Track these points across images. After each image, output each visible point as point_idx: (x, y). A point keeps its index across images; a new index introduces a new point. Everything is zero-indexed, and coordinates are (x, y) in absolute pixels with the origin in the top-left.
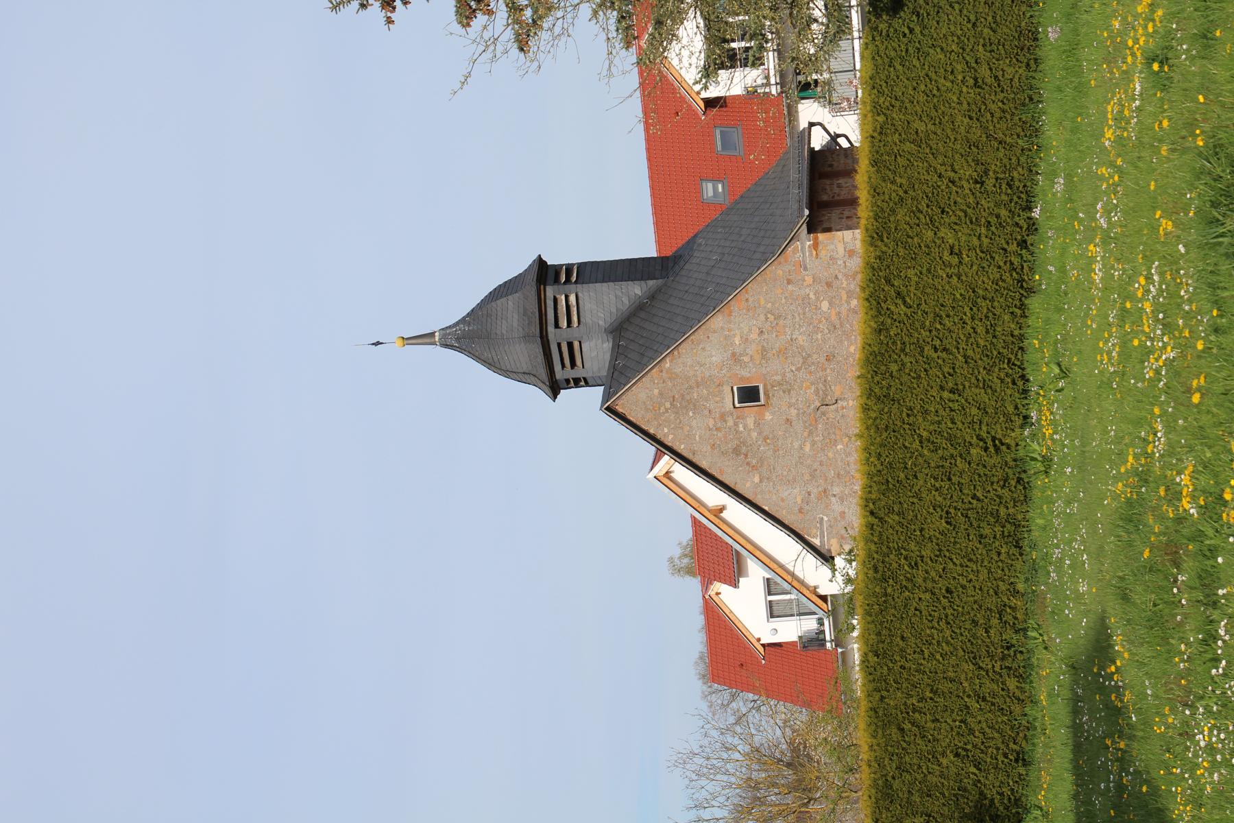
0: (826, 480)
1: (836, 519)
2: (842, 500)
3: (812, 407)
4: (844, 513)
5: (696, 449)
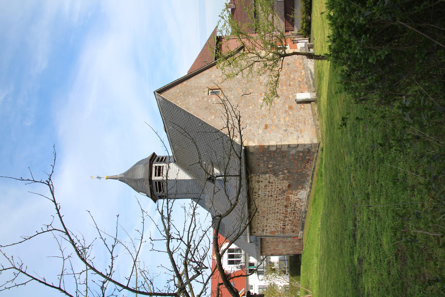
0: (244, 118)
1: (247, 132)
4: (251, 130)
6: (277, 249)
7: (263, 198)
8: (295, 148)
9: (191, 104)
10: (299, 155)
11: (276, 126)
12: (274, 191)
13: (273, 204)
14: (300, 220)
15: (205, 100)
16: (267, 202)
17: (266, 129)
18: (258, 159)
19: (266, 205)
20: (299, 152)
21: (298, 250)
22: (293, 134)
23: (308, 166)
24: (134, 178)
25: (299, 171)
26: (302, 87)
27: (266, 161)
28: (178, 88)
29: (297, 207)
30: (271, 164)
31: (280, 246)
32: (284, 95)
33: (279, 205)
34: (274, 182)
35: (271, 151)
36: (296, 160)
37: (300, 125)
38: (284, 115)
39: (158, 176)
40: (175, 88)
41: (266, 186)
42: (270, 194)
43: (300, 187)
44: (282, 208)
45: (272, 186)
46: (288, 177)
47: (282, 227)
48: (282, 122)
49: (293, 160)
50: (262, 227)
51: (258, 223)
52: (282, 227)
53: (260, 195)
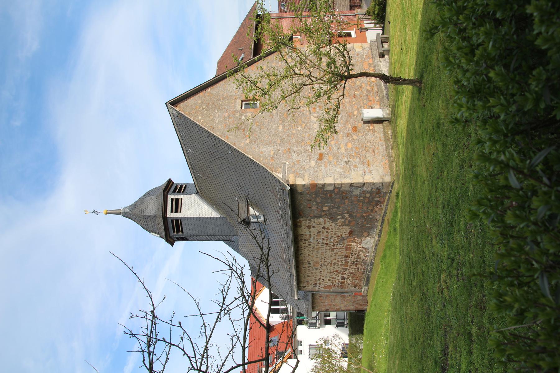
1: (294, 164)
2: (299, 154)
3: (286, 109)
4: (300, 161)
5: (215, 126)
6: (334, 303)
7: (316, 247)
8: (360, 187)
9: (217, 122)
10: (365, 196)
11: (335, 156)
12: (331, 238)
13: (329, 253)
14: (364, 273)
15: (236, 116)
16: (320, 251)
17: (320, 161)
18: (309, 200)
19: (319, 255)
20: (365, 192)
21: (361, 305)
22: (357, 168)
23: (377, 209)
24: (142, 214)
25: (364, 215)
26: (371, 99)
27: (319, 202)
28: (200, 98)
29: (360, 258)
30: (326, 206)
31: (337, 301)
32: (346, 110)
33: (337, 255)
34: (330, 227)
35: (326, 191)
36: (361, 202)
37: (368, 155)
38: (346, 140)
39: (175, 212)
40: (196, 97)
41: (319, 232)
42: (325, 242)
43: (366, 234)
44: (341, 259)
45: (327, 232)
46: (350, 222)
47: (340, 280)
48: (343, 150)
49: (356, 202)
50: (313, 280)
51: (309, 276)
52: (340, 280)
53: (311, 243)
